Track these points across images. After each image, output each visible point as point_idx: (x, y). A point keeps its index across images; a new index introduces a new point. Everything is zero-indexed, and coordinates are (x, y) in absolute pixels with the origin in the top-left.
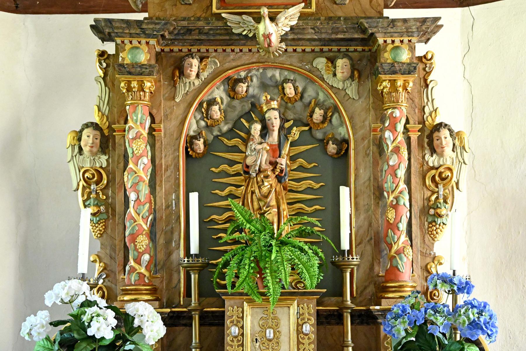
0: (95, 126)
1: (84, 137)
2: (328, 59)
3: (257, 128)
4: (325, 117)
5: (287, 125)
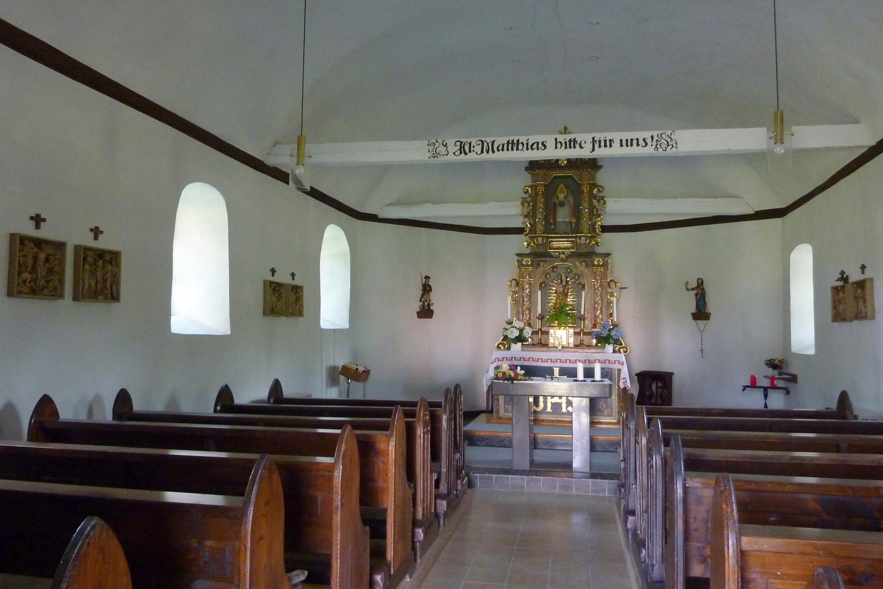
0: (515, 280)
1: (512, 283)
2: (579, 262)
3: (559, 281)
4: (579, 278)
5: (568, 279)
